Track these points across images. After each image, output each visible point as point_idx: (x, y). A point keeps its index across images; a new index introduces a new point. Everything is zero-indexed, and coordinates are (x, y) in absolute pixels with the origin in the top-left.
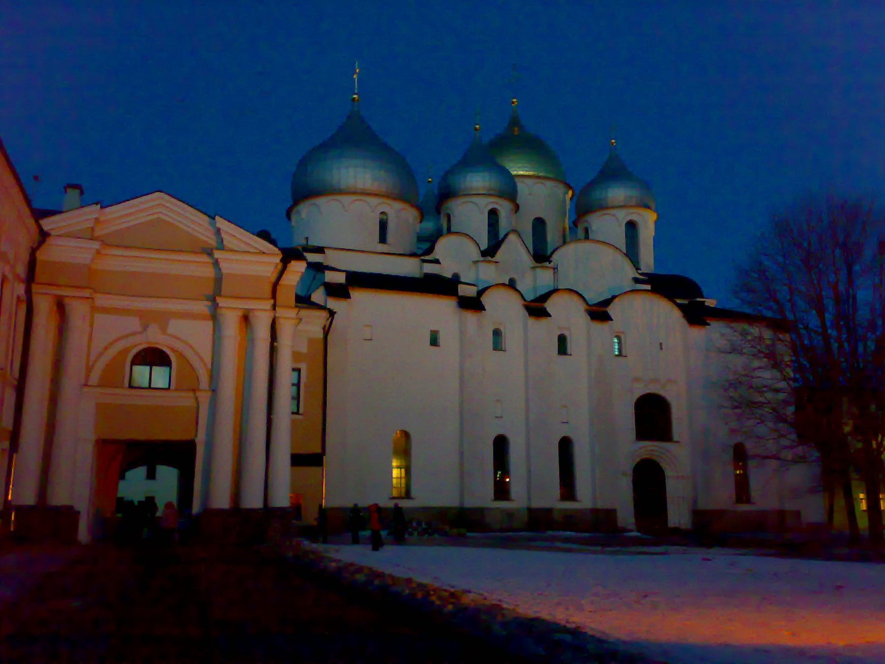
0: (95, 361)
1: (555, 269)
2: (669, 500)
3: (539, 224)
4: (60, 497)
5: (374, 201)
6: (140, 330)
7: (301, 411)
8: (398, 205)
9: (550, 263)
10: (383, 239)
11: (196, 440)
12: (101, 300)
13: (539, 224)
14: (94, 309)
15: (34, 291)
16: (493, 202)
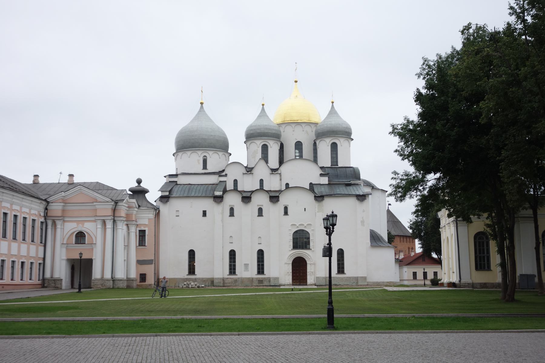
0: (65, 236)
1: (280, 174)
2: (308, 274)
3: (299, 145)
4: (56, 275)
5: (200, 153)
6: (76, 226)
7: (146, 245)
8: (211, 153)
9: (275, 172)
10: (205, 167)
11: (93, 258)
12: (66, 219)
13: (299, 145)
14: (64, 221)
15: (47, 218)
16: (263, 142)
